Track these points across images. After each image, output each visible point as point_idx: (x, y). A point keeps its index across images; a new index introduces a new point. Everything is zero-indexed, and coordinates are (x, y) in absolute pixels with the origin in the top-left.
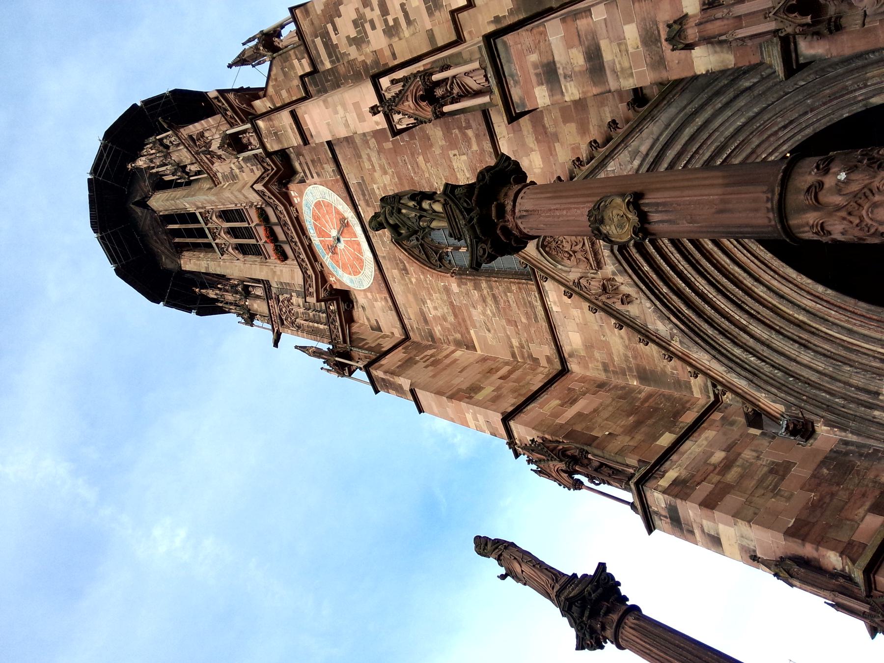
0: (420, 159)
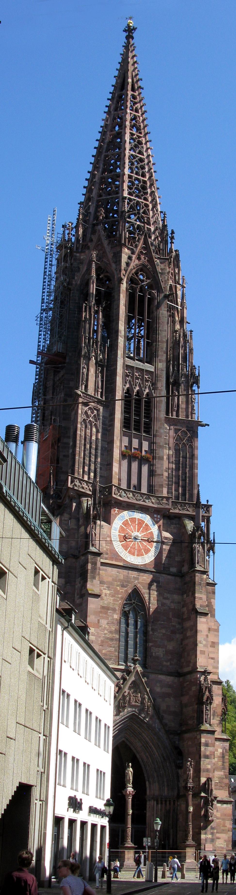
0: (164, 631)
